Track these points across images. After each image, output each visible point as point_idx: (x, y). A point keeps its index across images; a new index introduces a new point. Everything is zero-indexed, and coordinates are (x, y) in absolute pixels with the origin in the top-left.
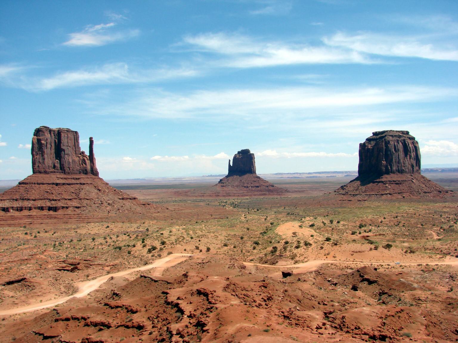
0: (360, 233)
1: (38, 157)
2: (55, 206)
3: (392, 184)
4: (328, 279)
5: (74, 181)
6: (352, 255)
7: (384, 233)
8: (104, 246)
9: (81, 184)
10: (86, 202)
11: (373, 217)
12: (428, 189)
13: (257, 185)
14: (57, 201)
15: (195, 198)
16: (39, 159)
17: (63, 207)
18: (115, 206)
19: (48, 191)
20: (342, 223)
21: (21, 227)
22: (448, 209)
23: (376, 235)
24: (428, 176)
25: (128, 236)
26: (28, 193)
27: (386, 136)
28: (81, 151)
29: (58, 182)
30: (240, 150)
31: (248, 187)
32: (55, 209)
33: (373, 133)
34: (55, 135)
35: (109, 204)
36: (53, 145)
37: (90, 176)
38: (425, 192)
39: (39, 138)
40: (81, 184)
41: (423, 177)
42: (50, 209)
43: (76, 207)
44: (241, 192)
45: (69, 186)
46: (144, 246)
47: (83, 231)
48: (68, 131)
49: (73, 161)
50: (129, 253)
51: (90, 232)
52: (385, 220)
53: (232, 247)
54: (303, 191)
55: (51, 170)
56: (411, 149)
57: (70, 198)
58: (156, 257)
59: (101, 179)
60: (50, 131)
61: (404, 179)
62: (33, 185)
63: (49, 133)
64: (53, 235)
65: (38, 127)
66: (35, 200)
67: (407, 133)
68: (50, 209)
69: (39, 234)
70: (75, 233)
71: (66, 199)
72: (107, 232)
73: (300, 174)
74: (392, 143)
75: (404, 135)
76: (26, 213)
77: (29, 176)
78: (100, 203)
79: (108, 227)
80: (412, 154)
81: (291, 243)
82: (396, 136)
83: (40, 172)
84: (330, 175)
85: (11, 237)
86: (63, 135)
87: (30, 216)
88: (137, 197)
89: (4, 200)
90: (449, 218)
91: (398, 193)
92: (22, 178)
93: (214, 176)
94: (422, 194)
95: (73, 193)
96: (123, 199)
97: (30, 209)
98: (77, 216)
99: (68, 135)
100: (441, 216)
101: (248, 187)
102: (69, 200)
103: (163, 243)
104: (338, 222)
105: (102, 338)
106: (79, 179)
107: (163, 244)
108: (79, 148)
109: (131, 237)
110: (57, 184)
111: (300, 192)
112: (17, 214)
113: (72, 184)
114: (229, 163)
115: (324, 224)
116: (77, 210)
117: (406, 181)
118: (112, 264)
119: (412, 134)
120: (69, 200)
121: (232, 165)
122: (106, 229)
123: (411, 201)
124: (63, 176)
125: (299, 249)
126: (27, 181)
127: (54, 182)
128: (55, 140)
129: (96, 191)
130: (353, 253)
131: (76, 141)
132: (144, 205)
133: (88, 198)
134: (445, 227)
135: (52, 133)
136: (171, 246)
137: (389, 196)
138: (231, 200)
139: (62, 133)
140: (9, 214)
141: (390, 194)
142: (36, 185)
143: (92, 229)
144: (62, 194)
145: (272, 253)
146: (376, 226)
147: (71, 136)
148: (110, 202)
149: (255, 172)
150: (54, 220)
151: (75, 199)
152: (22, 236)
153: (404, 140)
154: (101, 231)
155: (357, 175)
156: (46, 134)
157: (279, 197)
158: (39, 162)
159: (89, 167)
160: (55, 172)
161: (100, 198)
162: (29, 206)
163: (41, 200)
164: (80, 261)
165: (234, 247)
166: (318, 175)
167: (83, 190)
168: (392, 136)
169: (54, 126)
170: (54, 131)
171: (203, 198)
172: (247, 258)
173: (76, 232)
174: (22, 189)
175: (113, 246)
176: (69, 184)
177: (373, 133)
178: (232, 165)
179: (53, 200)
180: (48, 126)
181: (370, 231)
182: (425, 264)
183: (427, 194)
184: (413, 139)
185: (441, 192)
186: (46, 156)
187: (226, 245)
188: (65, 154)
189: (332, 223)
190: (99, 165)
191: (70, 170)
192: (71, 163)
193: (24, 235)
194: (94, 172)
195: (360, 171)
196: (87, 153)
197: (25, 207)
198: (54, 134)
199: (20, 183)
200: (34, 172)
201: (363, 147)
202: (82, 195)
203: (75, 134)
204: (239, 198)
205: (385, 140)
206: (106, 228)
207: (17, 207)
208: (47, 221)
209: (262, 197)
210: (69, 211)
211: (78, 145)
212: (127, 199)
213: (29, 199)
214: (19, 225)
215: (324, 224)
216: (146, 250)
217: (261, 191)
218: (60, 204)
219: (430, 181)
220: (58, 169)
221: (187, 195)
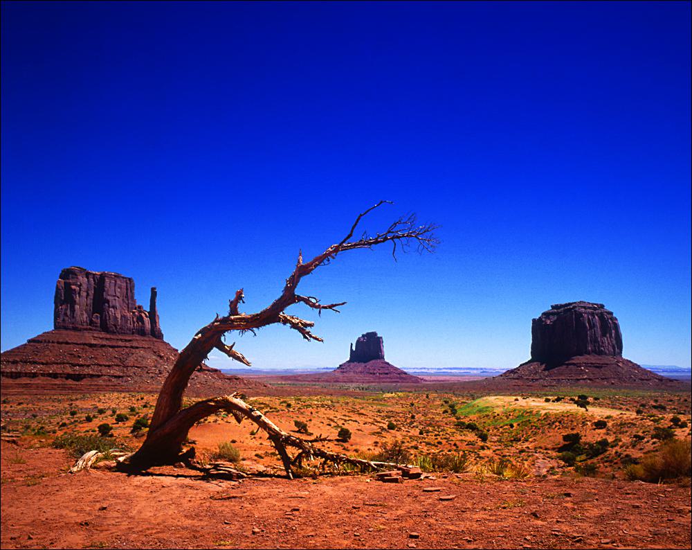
1: (64, 307)
2: (77, 373)
5: (120, 343)
9: (132, 347)
13: (387, 372)
14: (85, 367)
16: (66, 309)
28: (137, 304)
29: (93, 342)
32: (78, 377)
34: (94, 281)
36: (92, 292)
39: (67, 281)
40: (132, 347)
42: (68, 376)
49: (122, 316)
55: (85, 327)
60: (88, 275)
63: (85, 276)
68: (68, 376)
71: (101, 365)
83: (66, 328)
95: (115, 357)
99: (116, 281)
101: (374, 374)
102: (105, 366)
106: (130, 341)
108: (134, 301)
110: (91, 346)
114: (351, 347)
120: (105, 366)
124: (103, 335)
127: (87, 342)
128: (94, 287)
131: (129, 291)
135: (91, 276)
149: (383, 358)
156: (80, 278)
158: (66, 314)
159: (148, 326)
160: (90, 329)
163: (57, 364)
176: (112, 347)
186: (77, 307)
188: (109, 307)
190: (164, 325)
191: (116, 328)
192: (119, 319)
196: (147, 308)
198: (93, 278)
203: (128, 282)
211: (132, 297)
217: (390, 378)
218: (87, 371)
220: (96, 326)
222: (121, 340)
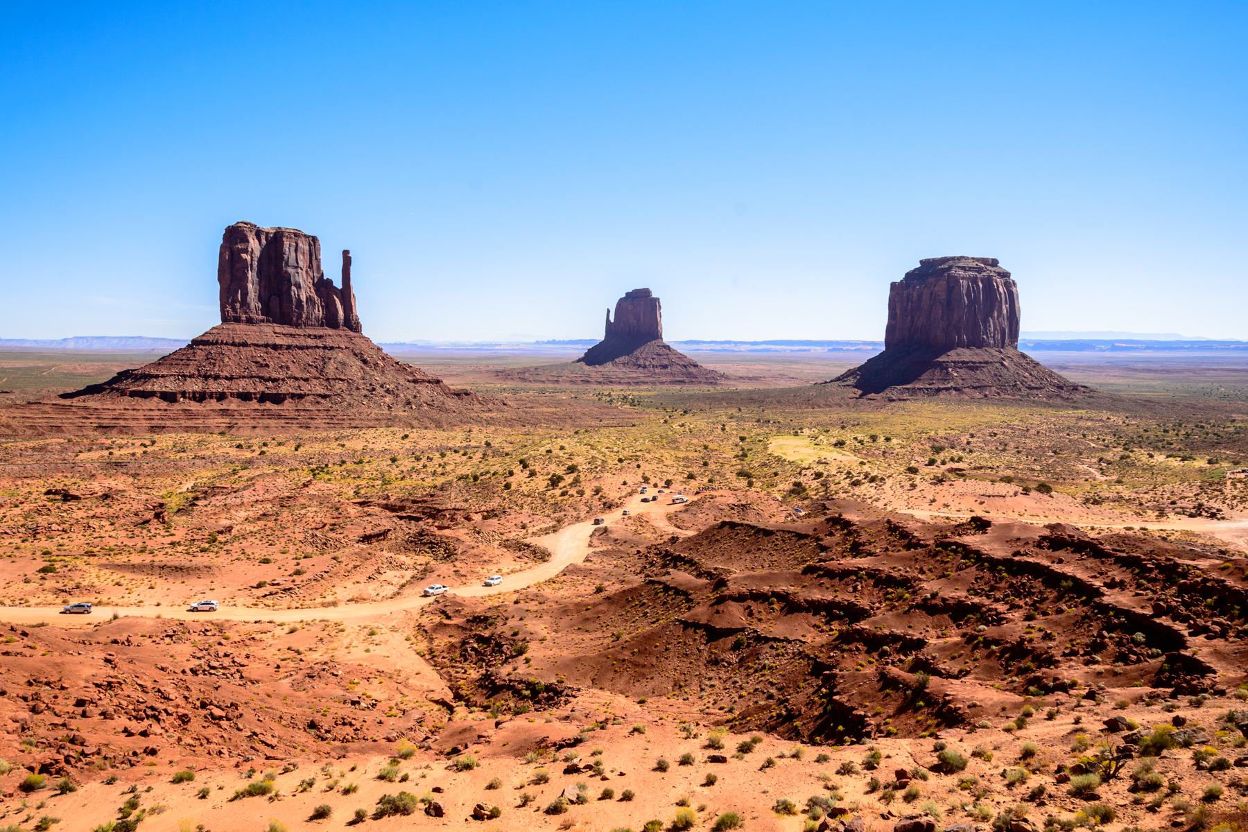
2: (274, 392)
3: (961, 368)
5: (310, 342)
6: (982, 503)
7: (990, 465)
8: (422, 475)
9: (325, 348)
10: (339, 385)
12: (1035, 381)
13: (665, 362)
15: (542, 386)
17: (293, 396)
18: (402, 395)
19: (259, 359)
20: (894, 441)
22: (1089, 424)
24: (1033, 355)
25: (464, 454)
26: (214, 365)
27: (950, 268)
29: (279, 341)
31: (645, 367)
33: (921, 262)
35: (388, 391)
37: (343, 331)
38: (1030, 388)
40: (325, 348)
41: (1024, 356)
42: (263, 398)
43: (320, 396)
44: (635, 375)
45: (300, 352)
46: (532, 474)
47: (358, 445)
48: (297, 235)
50: (508, 486)
51: (371, 446)
52: (975, 439)
53: (706, 480)
54: (756, 378)
56: (1003, 296)
57: (305, 376)
58: (573, 496)
59: (367, 340)
60: (258, 233)
61: (987, 359)
62: (225, 347)
64: (296, 450)
65: (232, 223)
66: (230, 379)
67: (994, 263)
68: (263, 398)
71: (296, 379)
72: (407, 446)
73: (736, 343)
74: (964, 283)
75: (990, 268)
76: (214, 404)
77: (213, 328)
78: (370, 388)
79: (406, 436)
80: (1004, 307)
81: (828, 476)
82: (970, 269)
83: (237, 320)
84: (797, 348)
85: (208, 453)
86: (286, 243)
87: (224, 413)
88: (440, 378)
89: (163, 376)
90: (1104, 440)
91: (974, 388)
92: (196, 334)
93: (559, 343)
94: (1025, 391)
96: (415, 381)
97: (221, 397)
98: (325, 413)
103: (572, 469)
104: (888, 440)
105: (895, 630)
106: (321, 337)
107: (572, 472)
109: (470, 458)
111: (750, 379)
112: (194, 406)
113: (308, 348)
115: (861, 442)
116: (322, 401)
117: (987, 363)
118: (483, 508)
119: (1004, 265)
121: (612, 321)
123: (1004, 403)
125: (863, 487)
126: (211, 338)
127: (270, 342)
129: (359, 363)
130: (983, 499)
132: (458, 395)
133: (343, 377)
134: (1109, 456)
135: (263, 237)
137: (954, 392)
138: (616, 391)
139: (284, 239)
140: (176, 406)
141: (956, 389)
142: (232, 348)
143: (374, 440)
144: (288, 368)
145: (799, 493)
147: (303, 245)
148: (391, 387)
150: (279, 421)
151: (316, 378)
152: (233, 452)
153: (989, 279)
154: (396, 446)
155: (883, 348)
156: (251, 240)
157: (711, 388)
161: (368, 377)
163: (244, 377)
164: (404, 503)
166: (773, 347)
167: (332, 361)
168: (963, 268)
169: (267, 226)
170: (267, 234)
171: (557, 386)
173: (343, 446)
174: (200, 354)
175: (443, 474)
176: (301, 348)
177: (921, 262)
178: (612, 321)
179: (270, 379)
180: (253, 223)
181: (960, 459)
183: (1035, 392)
184: (1005, 275)
185: (1061, 388)
187: (691, 477)
189: (874, 441)
190: (361, 310)
192: (304, 304)
193: (235, 449)
194: (352, 325)
195: (888, 342)
196: (338, 284)
197: (212, 393)
199: (196, 342)
200: (225, 319)
201: (897, 291)
202: (331, 369)
204: (631, 388)
205: (949, 275)
206: (403, 438)
207: (194, 393)
208: (267, 422)
209: (678, 387)
210: (307, 404)
212: (423, 381)
213: (217, 377)
214: (207, 430)
215: (861, 442)
216: (541, 483)
217: (672, 374)
218: (284, 389)
219: (1038, 364)
221: (524, 380)
222: (309, 336)
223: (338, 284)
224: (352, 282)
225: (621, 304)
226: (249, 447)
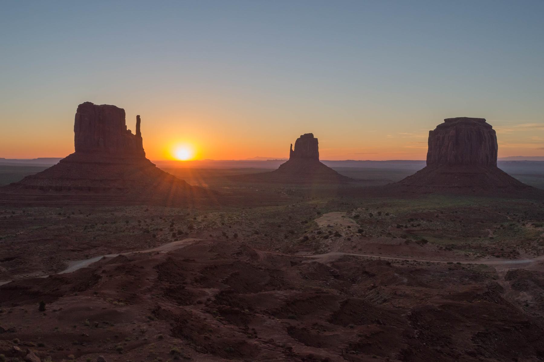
0: (406, 227)
4: (330, 270)
11: (429, 211)
21: (58, 207)
23: (424, 230)
28: (127, 129)
30: (303, 135)
33: (445, 120)
48: (114, 108)
50: (154, 236)
65: (82, 103)
69: (73, 215)
70: (111, 215)
79: (147, 210)
100: (508, 213)
109: (166, 221)
121: (293, 150)
122: (145, 213)
136: (198, 231)
146: (428, 220)
162: (69, 186)
165: (266, 235)
169: (98, 102)
172: (274, 246)
177: (445, 120)
178: (293, 150)
181: (419, 225)
182: (455, 262)
187: (257, 233)
196: (134, 132)
206: (145, 211)
223: (134, 132)
224: (142, 131)
225: (298, 141)
226: (65, 214)
